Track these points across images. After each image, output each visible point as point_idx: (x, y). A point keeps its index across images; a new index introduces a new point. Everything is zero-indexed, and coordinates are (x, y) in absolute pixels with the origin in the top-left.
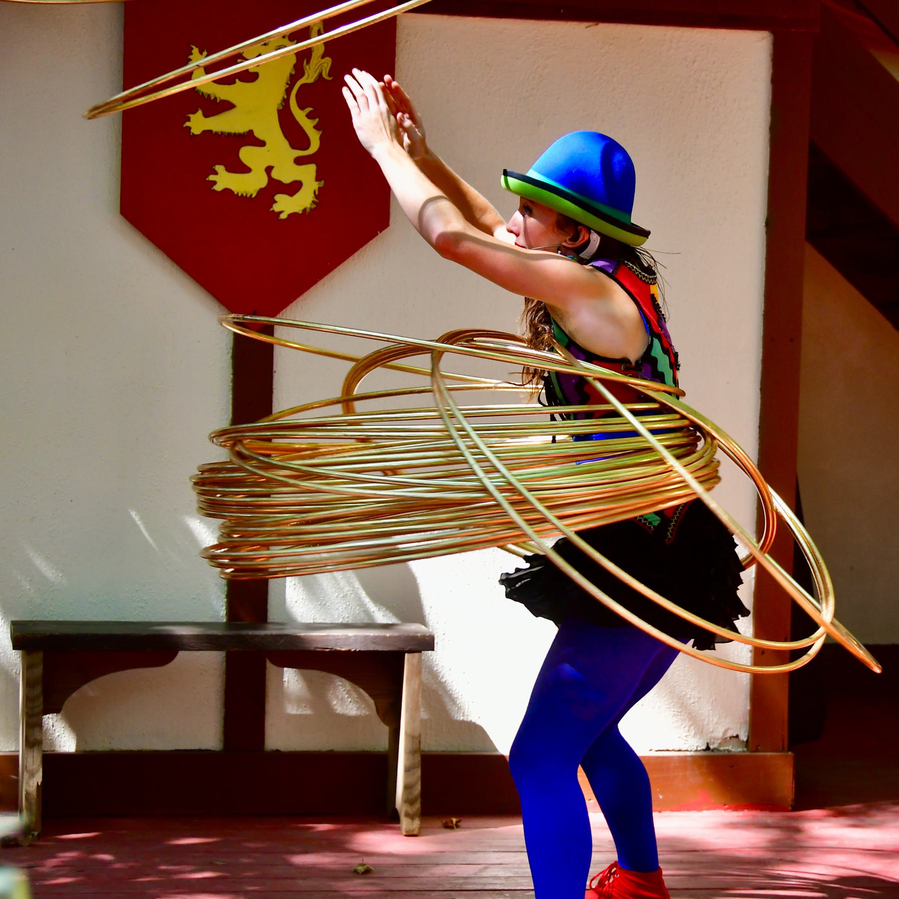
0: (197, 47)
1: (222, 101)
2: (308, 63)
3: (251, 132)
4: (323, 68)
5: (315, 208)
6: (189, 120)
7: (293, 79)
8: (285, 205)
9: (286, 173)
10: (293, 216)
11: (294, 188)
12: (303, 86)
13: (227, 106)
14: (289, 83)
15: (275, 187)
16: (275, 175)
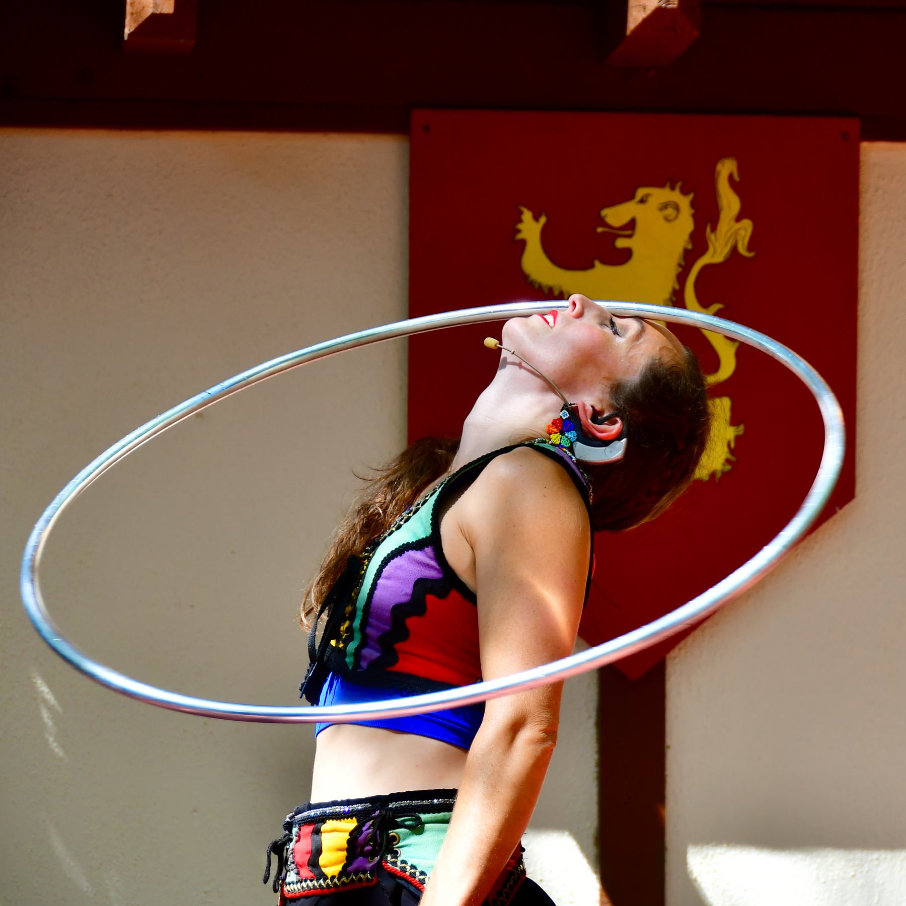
0: (529, 209)
2: (714, 229)
4: (739, 238)
5: (729, 472)
7: (689, 257)
12: (706, 268)
14: (683, 263)
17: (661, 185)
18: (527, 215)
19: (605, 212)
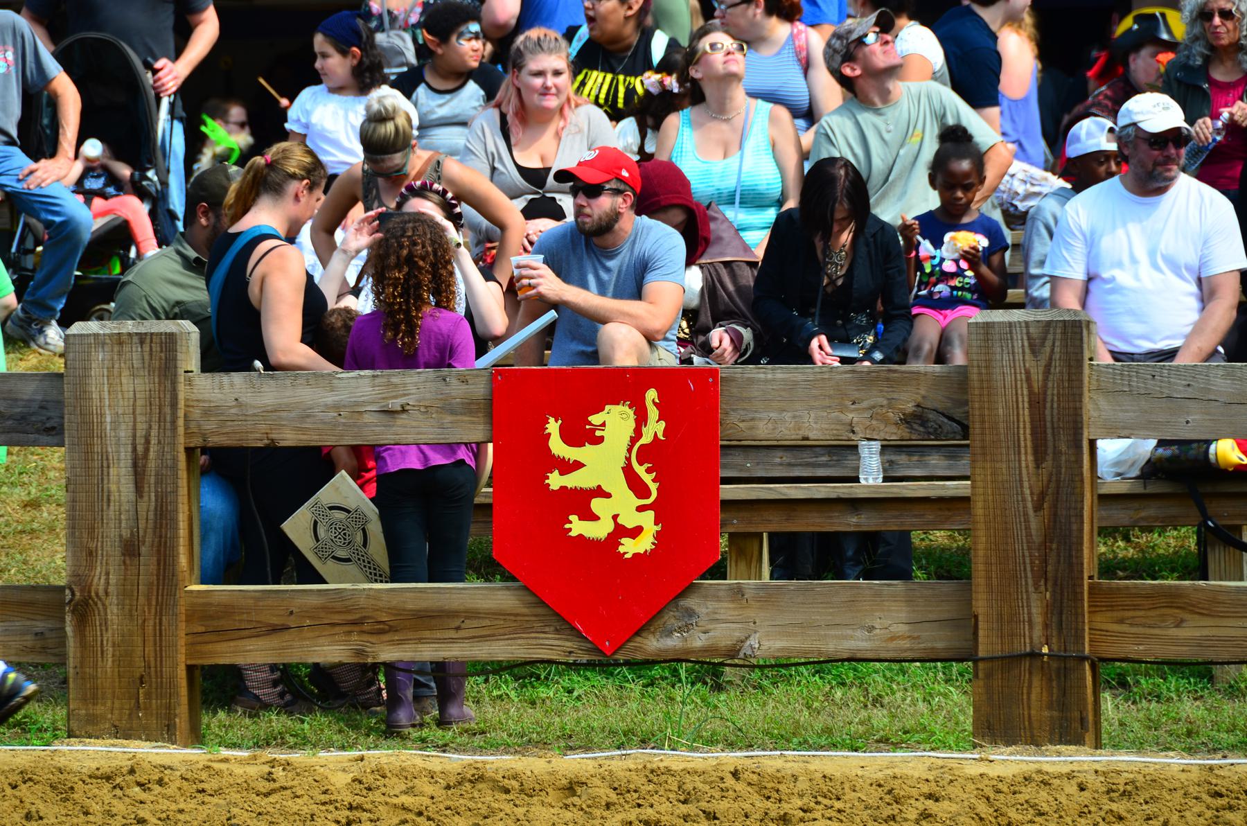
1: (575, 461)
3: (599, 487)
6: (548, 478)
7: (634, 440)
8: (629, 547)
9: (629, 521)
10: (636, 555)
11: (636, 532)
13: (578, 465)
15: (621, 532)
16: (620, 520)
17: (618, 404)
18: (552, 420)
19: (590, 418)
